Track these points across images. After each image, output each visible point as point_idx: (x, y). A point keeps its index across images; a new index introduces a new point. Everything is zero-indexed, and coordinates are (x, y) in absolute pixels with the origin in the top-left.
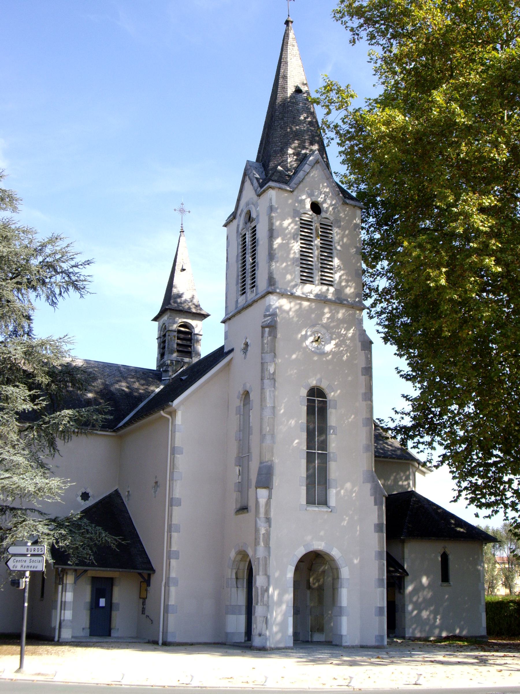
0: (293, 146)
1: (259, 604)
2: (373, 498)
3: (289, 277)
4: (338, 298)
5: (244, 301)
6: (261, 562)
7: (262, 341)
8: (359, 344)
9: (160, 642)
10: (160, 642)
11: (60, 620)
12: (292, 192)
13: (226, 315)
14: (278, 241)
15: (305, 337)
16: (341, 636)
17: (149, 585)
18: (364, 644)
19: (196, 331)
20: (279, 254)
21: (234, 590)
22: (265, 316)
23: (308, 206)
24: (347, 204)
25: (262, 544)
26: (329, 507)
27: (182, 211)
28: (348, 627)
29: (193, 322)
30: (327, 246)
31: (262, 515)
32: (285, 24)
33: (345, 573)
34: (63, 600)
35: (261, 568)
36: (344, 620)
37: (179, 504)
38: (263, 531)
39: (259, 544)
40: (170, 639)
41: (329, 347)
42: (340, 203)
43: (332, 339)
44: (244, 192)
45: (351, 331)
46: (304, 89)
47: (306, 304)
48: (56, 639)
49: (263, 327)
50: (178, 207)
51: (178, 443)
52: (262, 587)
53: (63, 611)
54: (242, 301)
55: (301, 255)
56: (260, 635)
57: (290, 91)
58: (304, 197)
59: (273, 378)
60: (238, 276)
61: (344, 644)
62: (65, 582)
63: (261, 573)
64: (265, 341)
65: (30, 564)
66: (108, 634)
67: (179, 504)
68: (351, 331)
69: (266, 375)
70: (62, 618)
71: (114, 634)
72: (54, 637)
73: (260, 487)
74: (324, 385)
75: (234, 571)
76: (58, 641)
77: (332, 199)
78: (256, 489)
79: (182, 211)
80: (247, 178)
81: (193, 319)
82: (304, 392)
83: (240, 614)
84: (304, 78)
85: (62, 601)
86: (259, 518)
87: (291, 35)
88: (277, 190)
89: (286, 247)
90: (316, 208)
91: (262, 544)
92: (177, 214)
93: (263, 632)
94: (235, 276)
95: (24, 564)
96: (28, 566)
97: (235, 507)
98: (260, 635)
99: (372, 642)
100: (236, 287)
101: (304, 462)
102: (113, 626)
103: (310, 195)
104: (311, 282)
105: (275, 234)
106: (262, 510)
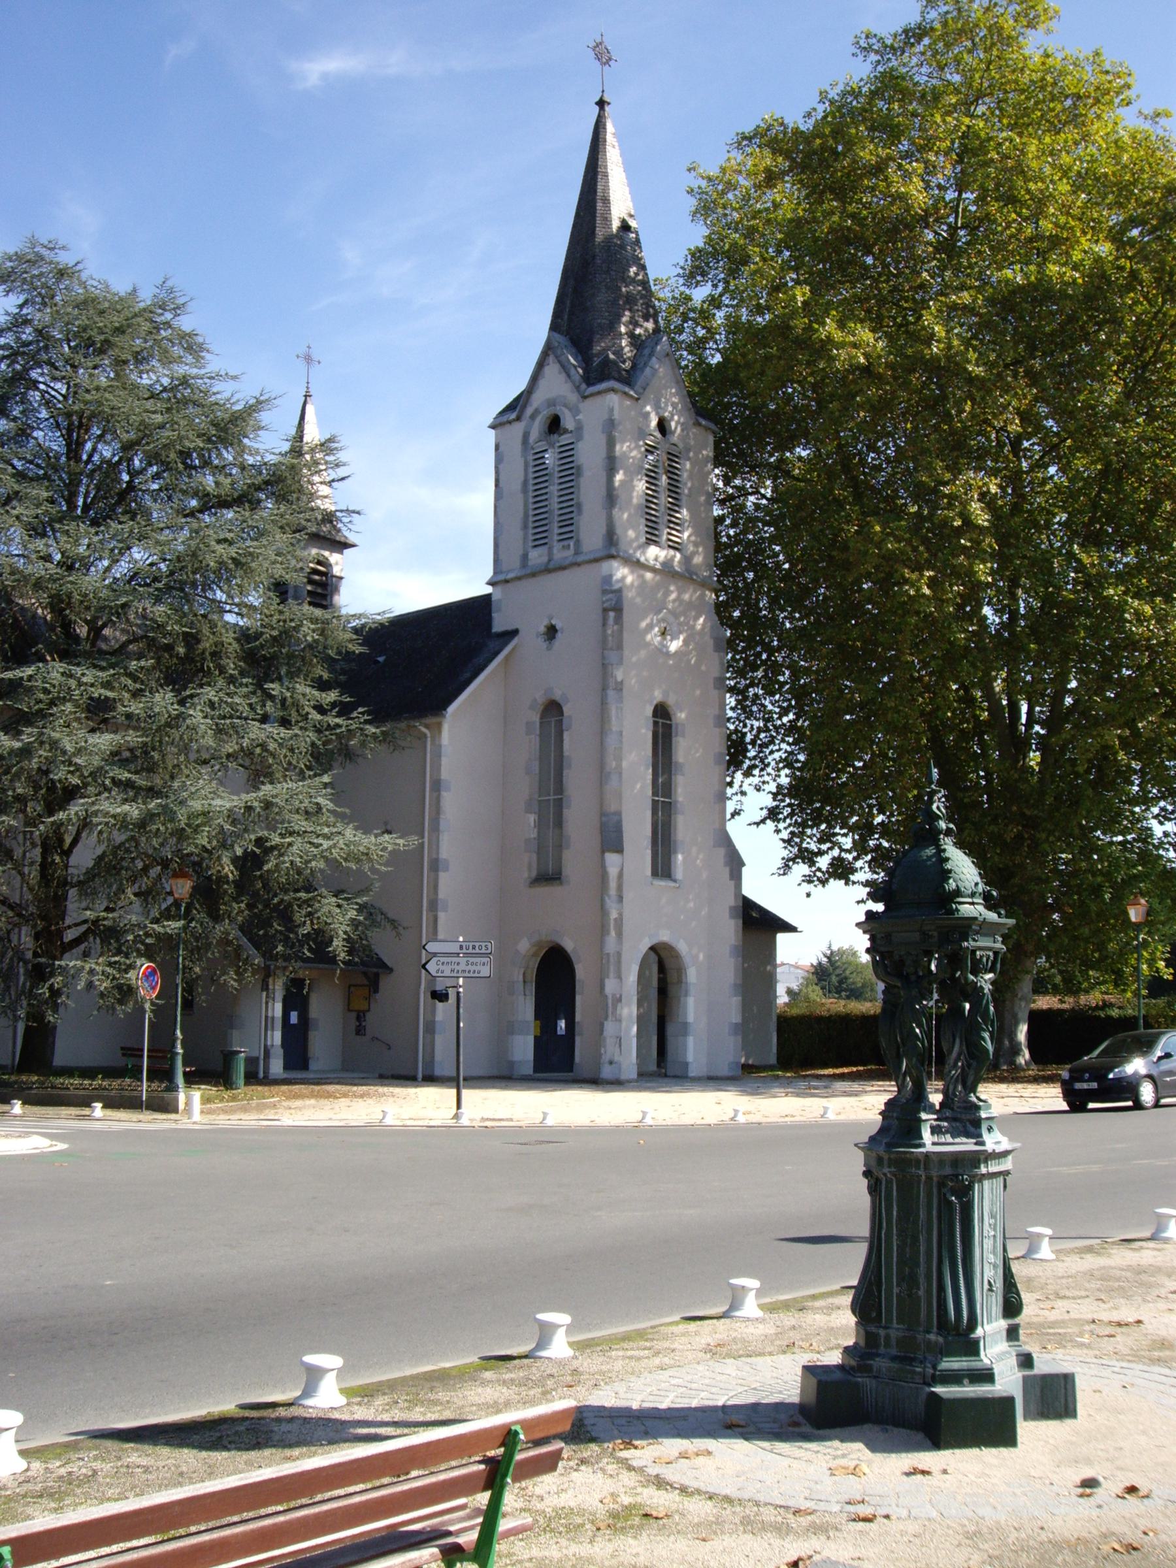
0: (624, 319)
1: (610, 1018)
2: (727, 869)
3: (631, 534)
4: (687, 570)
5: (545, 559)
6: (612, 960)
7: (604, 631)
8: (711, 642)
9: (420, 1076)
10: (420, 1076)
11: (266, 1046)
12: (637, 399)
13: (495, 573)
14: (619, 477)
15: (650, 627)
16: (687, 1064)
17: (376, 991)
18: (711, 1074)
19: (336, 571)
20: (622, 496)
21: (521, 998)
22: (605, 592)
23: (654, 423)
24: (700, 424)
25: (613, 933)
26: (675, 881)
27: (308, 359)
28: (693, 1050)
29: (334, 558)
30: (674, 488)
31: (613, 891)
32: (597, 103)
33: (692, 975)
34: (270, 1014)
35: (612, 968)
36: (690, 1040)
37: (447, 869)
38: (614, 915)
39: (608, 933)
40: (438, 1072)
41: (674, 646)
42: (691, 422)
43: (681, 632)
44: (542, 383)
45: (701, 620)
46: (633, 223)
47: (649, 575)
48: (261, 1075)
49: (605, 611)
50: (302, 350)
51: (445, 775)
52: (614, 995)
53: (269, 1033)
54: (537, 557)
55: (647, 501)
56: (611, 1063)
57: (616, 225)
58: (648, 408)
59: (619, 687)
60: (526, 515)
61: (691, 1074)
62: (271, 987)
63: (612, 975)
64: (609, 632)
65: (468, 968)
66: (304, 1066)
67: (447, 869)
68: (701, 620)
69: (612, 684)
70: (269, 1043)
71: (313, 1065)
72: (257, 1073)
73: (609, 851)
74: (671, 701)
75: (522, 971)
76: (266, 1077)
77: (680, 414)
78: (603, 852)
79: (308, 359)
80: (551, 358)
81: (332, 551)
82: (649, 710)
83: (528, 1034)
84: (631, 205)
85: (267, 1017)
86: (609, 896)
87: (610, 128)
88: (619, 394)
89: (628, 484)
90: (662, 426)
91: (613, 933)
92: (301, 365)
93: (616, 1058)
94: (521, 514)
95: (457, 968)
96: (464, 971)
97: (526, 875)
98: (611, 1063)
99: (725, 1072)
100: (521, 533)
101: (649, 813)
102: (310, 1054)
103: (657, 407)
104: (656, 543)
105: (618, 465)
106: (613, 884)
